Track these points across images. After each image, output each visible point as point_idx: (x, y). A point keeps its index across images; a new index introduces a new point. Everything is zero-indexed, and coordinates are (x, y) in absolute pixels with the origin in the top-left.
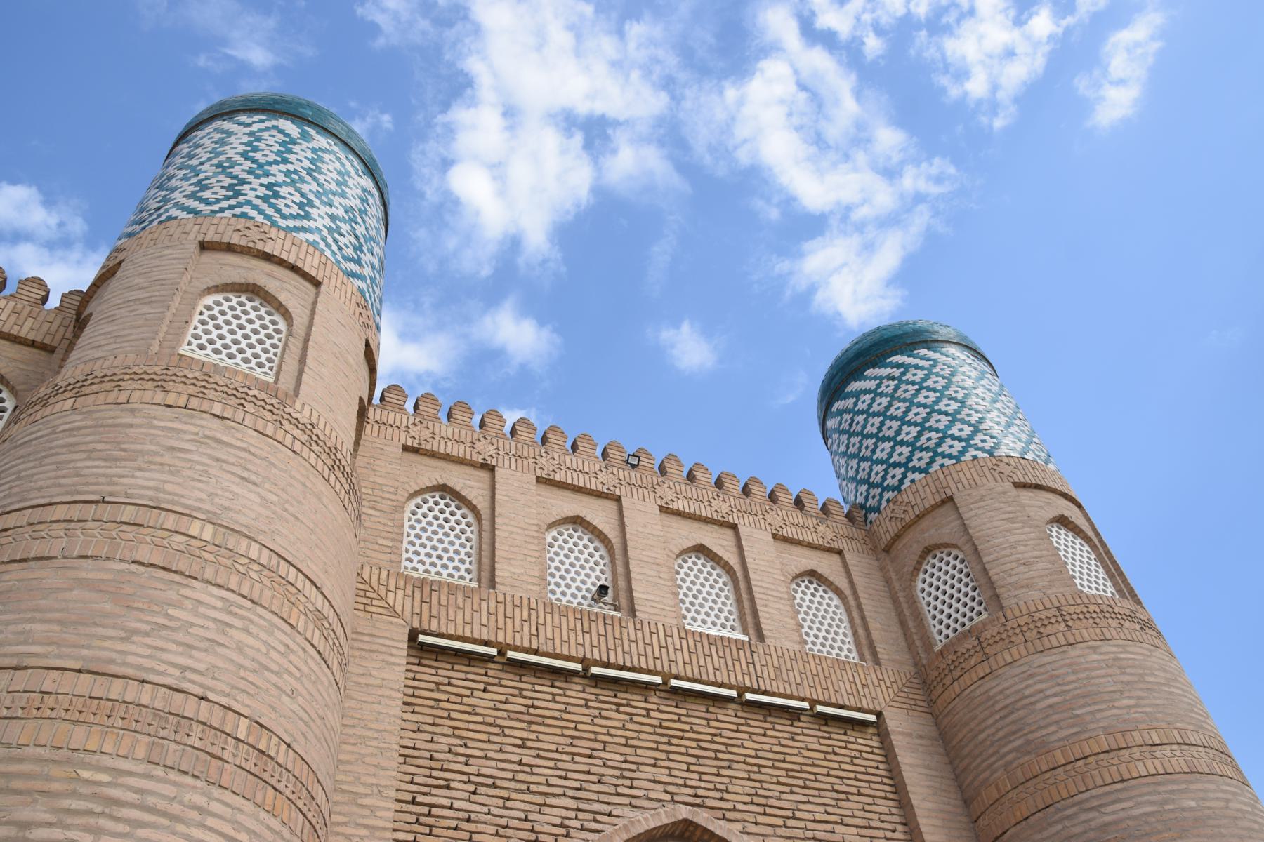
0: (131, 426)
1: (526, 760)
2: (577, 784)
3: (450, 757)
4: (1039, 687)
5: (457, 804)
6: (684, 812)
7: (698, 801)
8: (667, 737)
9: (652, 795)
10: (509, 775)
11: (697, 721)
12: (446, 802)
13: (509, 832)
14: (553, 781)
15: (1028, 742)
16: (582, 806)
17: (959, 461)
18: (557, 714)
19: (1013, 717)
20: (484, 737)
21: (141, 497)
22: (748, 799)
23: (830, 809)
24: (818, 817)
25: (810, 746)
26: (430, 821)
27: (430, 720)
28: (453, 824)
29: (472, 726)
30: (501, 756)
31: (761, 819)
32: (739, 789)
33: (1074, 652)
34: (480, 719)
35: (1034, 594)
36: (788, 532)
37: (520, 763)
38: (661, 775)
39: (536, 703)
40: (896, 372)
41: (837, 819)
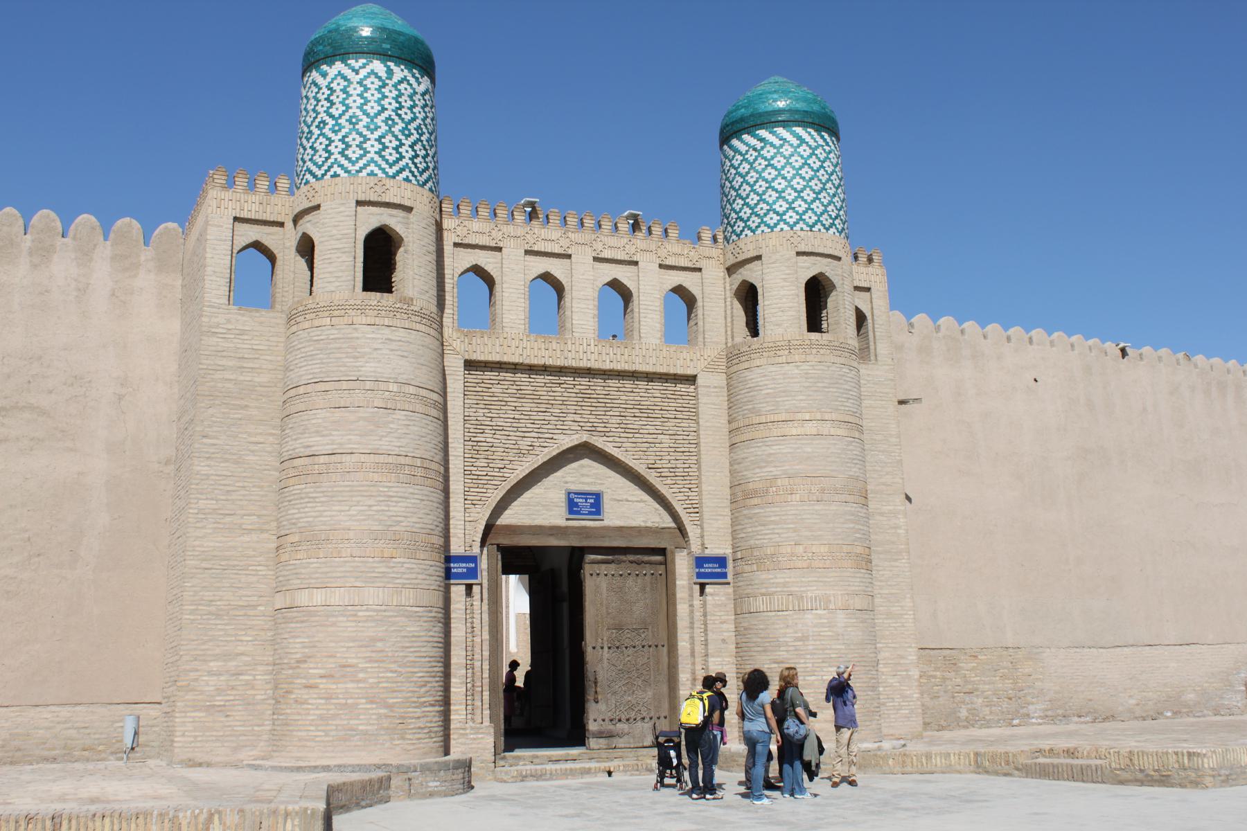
6: (585, 437)
8: (585, 396)
33: (787, 367)
35: (780, 331)
36: (669, 262)
38: (577, 418)
40: (759, 145)
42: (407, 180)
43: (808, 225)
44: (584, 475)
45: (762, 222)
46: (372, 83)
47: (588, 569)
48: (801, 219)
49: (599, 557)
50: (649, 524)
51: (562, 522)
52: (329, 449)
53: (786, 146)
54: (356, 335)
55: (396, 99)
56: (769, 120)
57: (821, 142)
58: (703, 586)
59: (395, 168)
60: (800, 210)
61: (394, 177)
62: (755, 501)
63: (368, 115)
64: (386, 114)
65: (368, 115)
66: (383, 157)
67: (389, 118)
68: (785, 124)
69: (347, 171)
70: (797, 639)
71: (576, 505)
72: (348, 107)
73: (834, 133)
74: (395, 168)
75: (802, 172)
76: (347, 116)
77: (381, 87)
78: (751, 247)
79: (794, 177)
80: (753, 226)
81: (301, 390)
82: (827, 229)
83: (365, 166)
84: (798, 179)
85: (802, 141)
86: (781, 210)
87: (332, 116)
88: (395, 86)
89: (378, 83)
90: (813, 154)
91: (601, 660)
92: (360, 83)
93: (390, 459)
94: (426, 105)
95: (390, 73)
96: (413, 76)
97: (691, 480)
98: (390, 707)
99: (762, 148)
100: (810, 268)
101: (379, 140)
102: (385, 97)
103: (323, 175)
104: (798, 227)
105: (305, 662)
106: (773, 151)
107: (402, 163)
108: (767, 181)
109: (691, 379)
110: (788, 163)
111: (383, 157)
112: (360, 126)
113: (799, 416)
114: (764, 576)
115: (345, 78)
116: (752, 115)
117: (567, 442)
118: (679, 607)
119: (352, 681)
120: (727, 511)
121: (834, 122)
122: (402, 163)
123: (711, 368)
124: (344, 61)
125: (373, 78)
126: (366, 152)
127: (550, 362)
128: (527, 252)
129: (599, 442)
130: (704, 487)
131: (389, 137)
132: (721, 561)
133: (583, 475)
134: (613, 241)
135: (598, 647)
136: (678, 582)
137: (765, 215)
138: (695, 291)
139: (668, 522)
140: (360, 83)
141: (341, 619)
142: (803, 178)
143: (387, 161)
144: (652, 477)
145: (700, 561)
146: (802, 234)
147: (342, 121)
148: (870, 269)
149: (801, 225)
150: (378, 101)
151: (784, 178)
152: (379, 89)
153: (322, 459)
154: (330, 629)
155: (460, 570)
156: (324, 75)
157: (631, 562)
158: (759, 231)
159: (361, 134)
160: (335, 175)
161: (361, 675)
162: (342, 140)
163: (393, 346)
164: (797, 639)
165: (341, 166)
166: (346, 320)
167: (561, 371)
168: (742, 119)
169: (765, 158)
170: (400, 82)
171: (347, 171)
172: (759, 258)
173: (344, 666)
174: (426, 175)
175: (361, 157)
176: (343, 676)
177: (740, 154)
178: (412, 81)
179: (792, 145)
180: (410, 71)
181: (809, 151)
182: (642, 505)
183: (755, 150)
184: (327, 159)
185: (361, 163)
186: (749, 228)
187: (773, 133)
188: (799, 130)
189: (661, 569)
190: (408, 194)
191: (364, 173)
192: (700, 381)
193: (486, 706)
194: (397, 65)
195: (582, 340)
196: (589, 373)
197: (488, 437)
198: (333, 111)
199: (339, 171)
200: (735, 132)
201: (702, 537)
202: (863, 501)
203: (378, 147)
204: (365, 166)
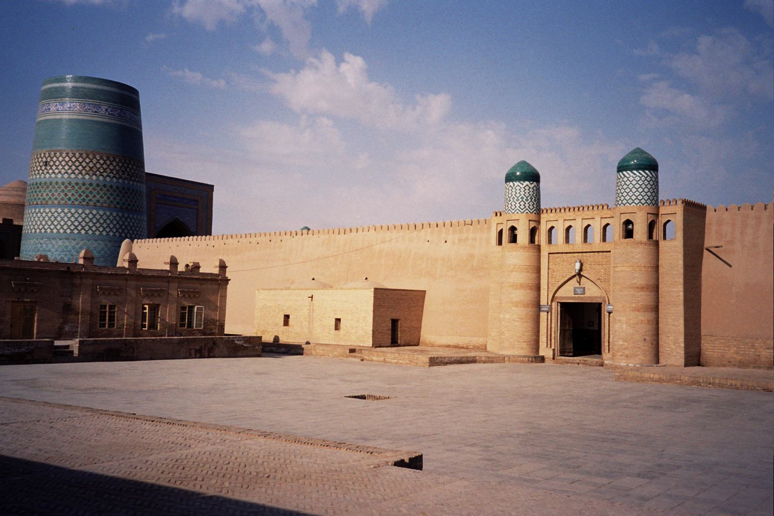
66: (520, 208)
67: (522, 197)
82: (630, 204)
111: (520, 208)
146: (622, 207)
165: (519, 210)
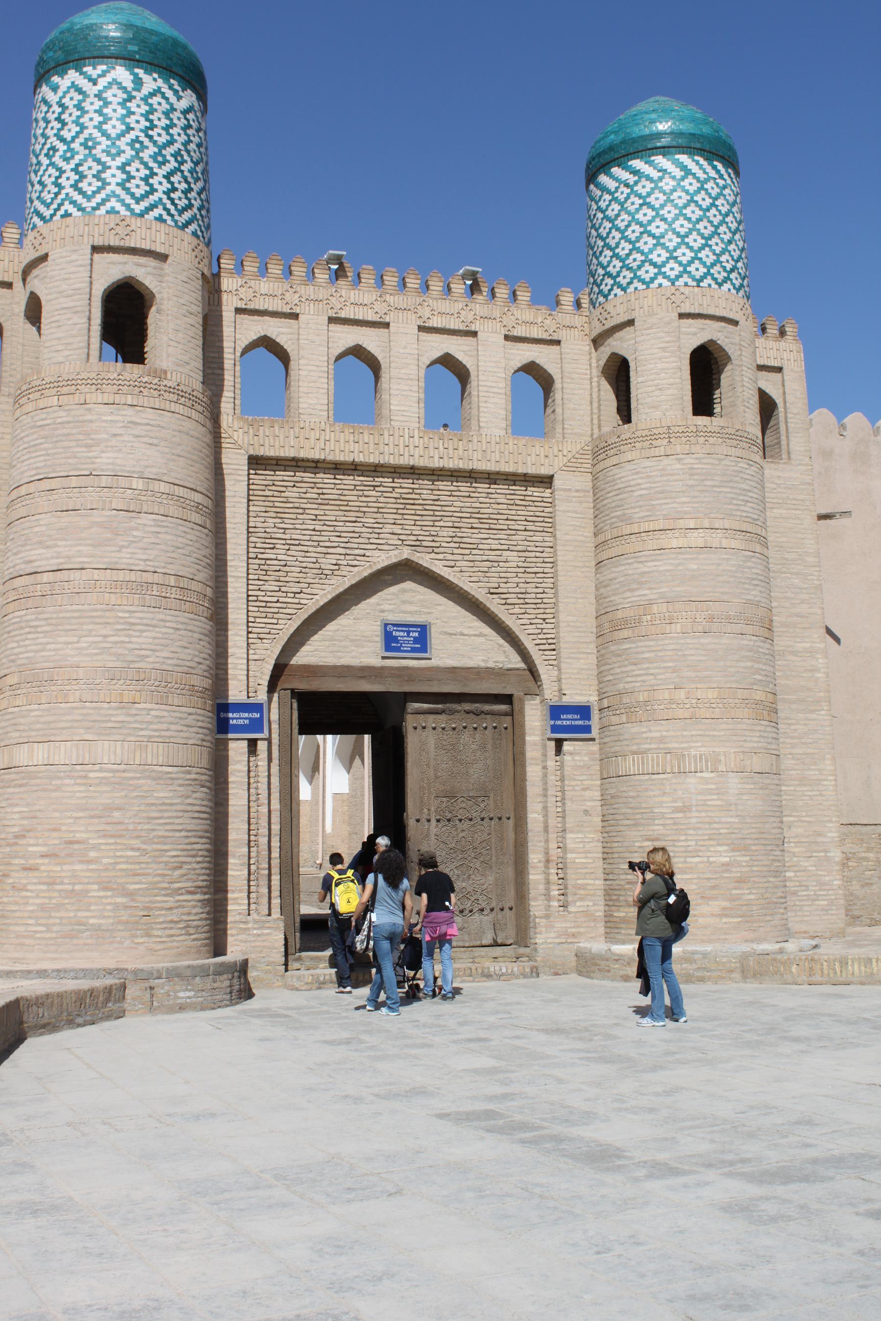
0: (91, 421)
1: (317, 528)
2: (346, 540)
3: (275, 530)
4: (639, 481)
5: (280, 557)
6: (406, 553)
7: (418, 543)
8: (406, 502)
9: (391, 542)
10: (308, 538)
11: (425, 492)
12: (274, 557)
13: (307, 570)
14: (332, 539)
15: (624, 514)
16: (348, 552)
17: (648, 287)
18: (336, 497)
19: (621, 496)
20: (294, 516)
21: (108, 470)
22: (449, 539)
23: (502, 542)
24: (493, 547)
25: (499, 501)
26: (266, 567)
27: (263, 509)
28: (278, 568)
29: (287, 510)
30: (304, 527)
31: (456, 551)
32: (445, 534)
33: (666, 461)
34: (291, 505)
35: (658, 414)
36: (519, 332)
37: (314, 530)
38: (397, 529)
39: (325, 491)
40: (632, 179)
41: (506, 547)
42: (160, 219)
43: (694, 279)
44: (406, 602)
45: (635, 276)
46: (114, 96)
47: (410, 722)
48: (685, 271)
49: (426, 706)
50: (491, 664)
51: (376, 661)
52: (53, 564)
53: (667, 179)
54: (89, 417)
55: (146, 116)
56: (645, 147)
57: (713, 174)
58: (559, 743)
59: (144, 205)
60: (684, 260)
61: (141, 215)
62: (625, 633)
63: (108, 137)
64: (132, 135)
65: (108, 137)
66: (127, 190)
67: (137, 140)
68: (665, 151)
69: (81, 209)
70: (677, 810)
71: (396, 640)
72: (83, 128)
73: (731, 162)
74: (144, 205)
75: (688, 211)
76: (81, 139)
77: (126, 101)
78: (621, 309)
79: (676, 218)
80: (624, 282)
81: (23, 490)
82: (720, 285)
83: (104, 202)
84: (681, 221)
85: (687, 172)
86: (659, 261)
87: (63, 140)
88: (145, 99)
89: (122, 96)
90: (702, 188)
91: (428, 835)
92: (99, 96)
93: (132, 576)
94: (189, 126)
95: (138, 83)
96: (171, 87)
97: (545, 608)
98: (130, 895)
99: (636, 183)
100: (697, 334)
101: (122, 168)
102: (130, 113)
103: (52, 216)
104: (680, 282)
105: (24, 836)
106: (649, 186)
107: (153, 198)
108: (641, 224)
109: (546, 481)
110: (669, 200)
112: (97, 152)
113: (682, 523)
114: (634, 730)
115: (80, 91)
116: (623, 142)
117: (382, 559)
118: (529, 769)
119: (81, 862)
120: (592, 648)
121: (730, 148)
122: (153, 198)
123: (569, 468)
124: (78, 69)
125: (115, 90)
126: (105, 184)
127: (360, 458)
128: (332, 320)
129: (425, 560)
130: (562, 617)
131: (136, 164)
132: (584, 711)
133: (404, 602)
134: (444, 306)
135: (423, 820)
136: (528, 738)
137: (639, 267)
138: (552, 368)
139: (515, 661)
140: (99, 96)
141: (67, 781)
142: (689, 220)
143: (133, 195)
144: (494, 605)
145: (556, 711)
146: (686, 290)
147: (75, 146)
148: (782, 344)
149: (685, 278)
150: (122, 119)
151: (664, 219)
152: (123, 104)
153: (45, 577)
154: (54, 794)
155: (241, 722)
156: (55, 89)
157: (468, 712)
158: (631, 289)
159: (98, 161)
160: (67, 215)
161: (93, 854)
162: (75, 170)
163: (138, 431)
164: (677, 810)
166: (77, 398)
167: (376, 470)
168: (611, 148)
169: (640, 196)
170: (152, 94)
171: (81, 209)
172: (631, 323)
173: (71, 842)
174: (187, 215)
175: (99, 190)
176: (69, 855)
177: (609, 192)
178: (169, 94)
179: (674, 178)
180: (166, 81)
181: (696, 185)
182: (482, 639)
183: (627, 185)
184: (56, 195)
185: (98, 198)
186: (620, 286)
187: (650, 163)
188: (684, 158)
189: (507, 722)
190: (161, 237)
191: (103, 210)
192: (557, 482)
193: (276, 893)
194: (148, 72)
195: (403, 427)
196: (413, 472)
197: (280, 552)
198: (65, 133)
199: (71, 209)
200: (603, 166)
201: (559, 680)
202: (766, 633)
203: (120, 176)
204: (104, 202)
